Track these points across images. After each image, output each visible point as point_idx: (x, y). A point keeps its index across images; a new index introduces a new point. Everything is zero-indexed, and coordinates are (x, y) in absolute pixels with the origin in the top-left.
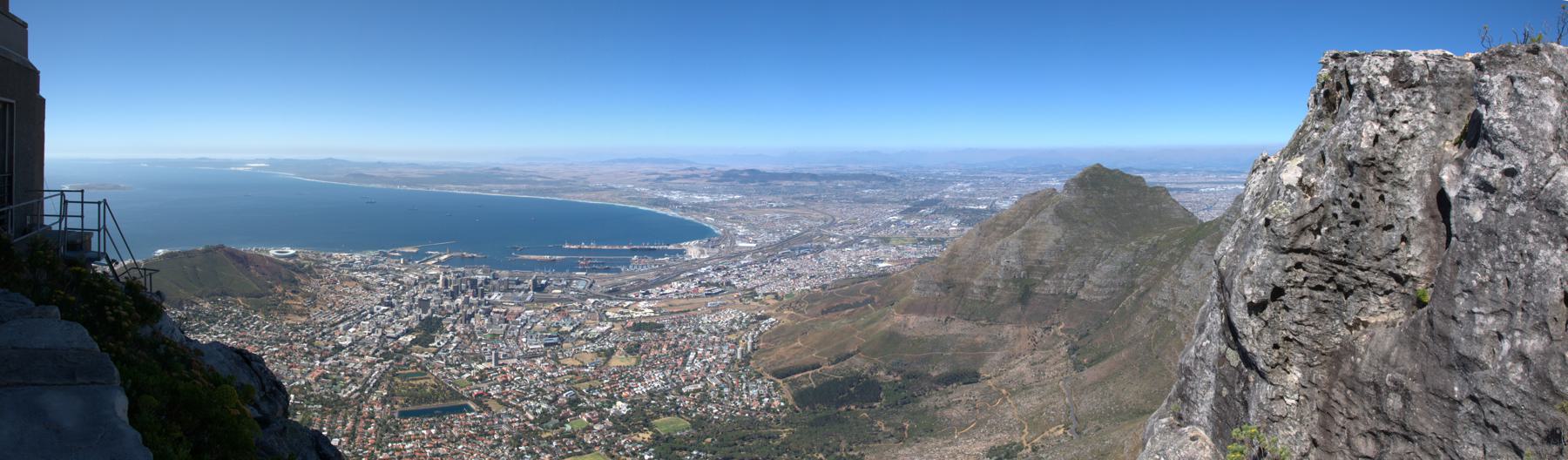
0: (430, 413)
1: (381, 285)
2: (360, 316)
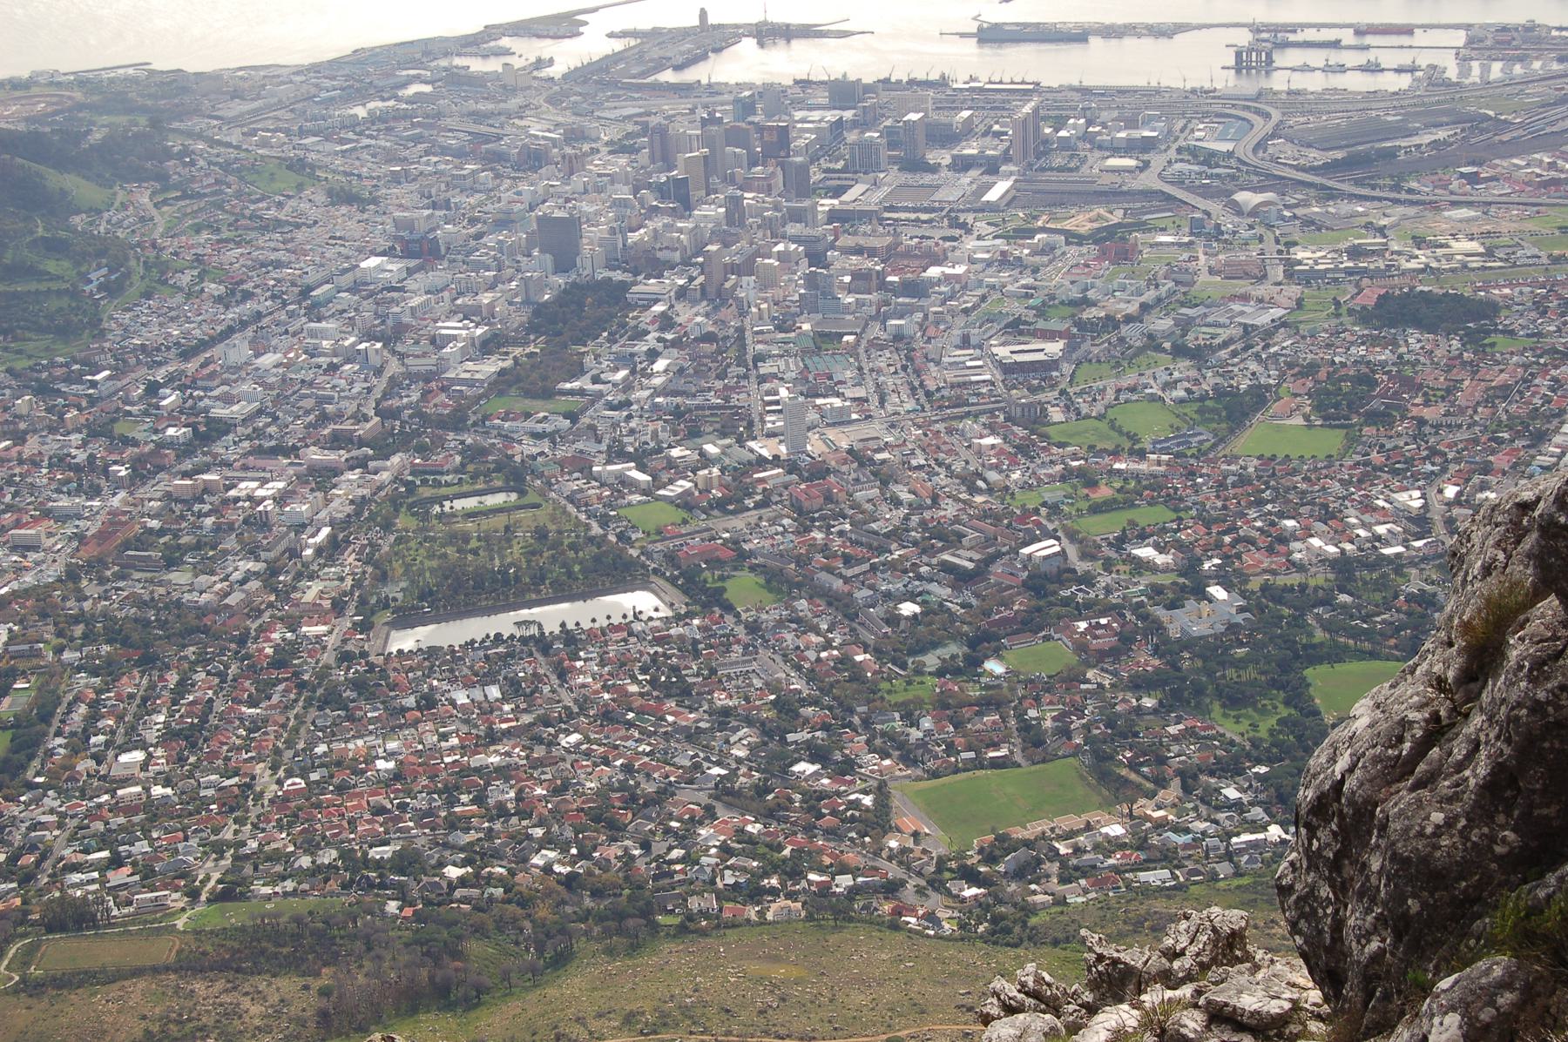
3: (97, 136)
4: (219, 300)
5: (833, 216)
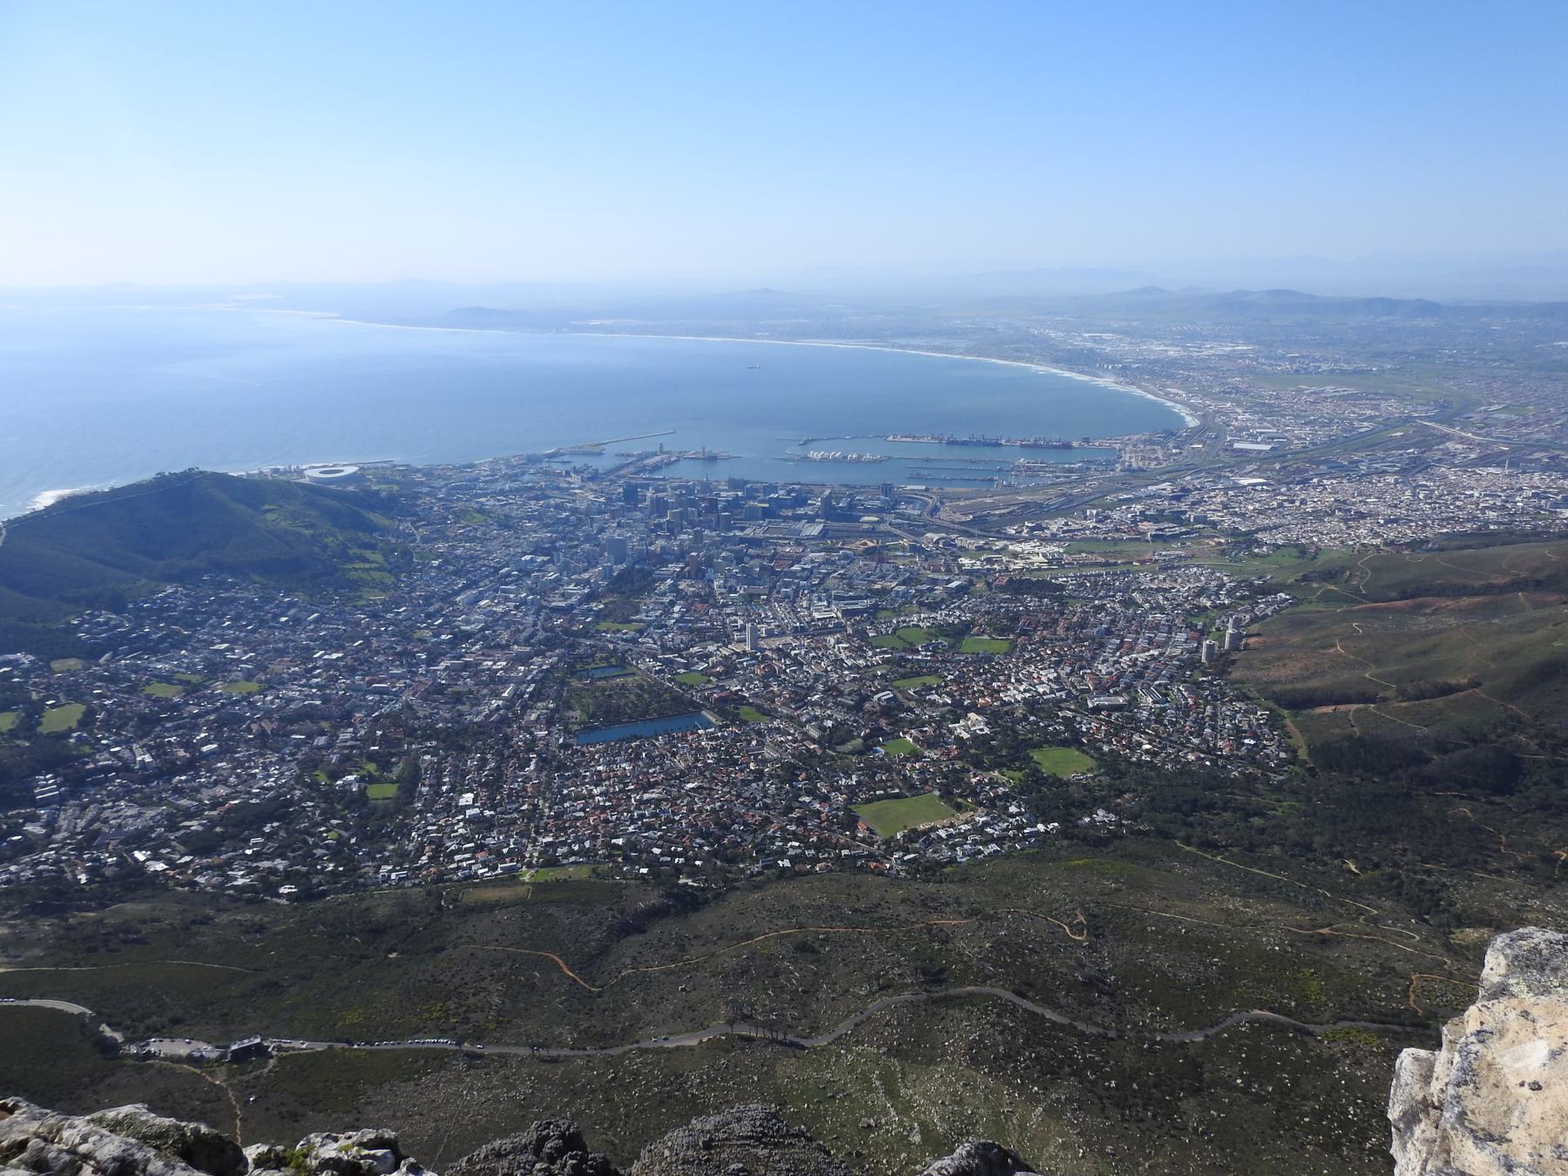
3: (384, 494)
5: (742, 540)
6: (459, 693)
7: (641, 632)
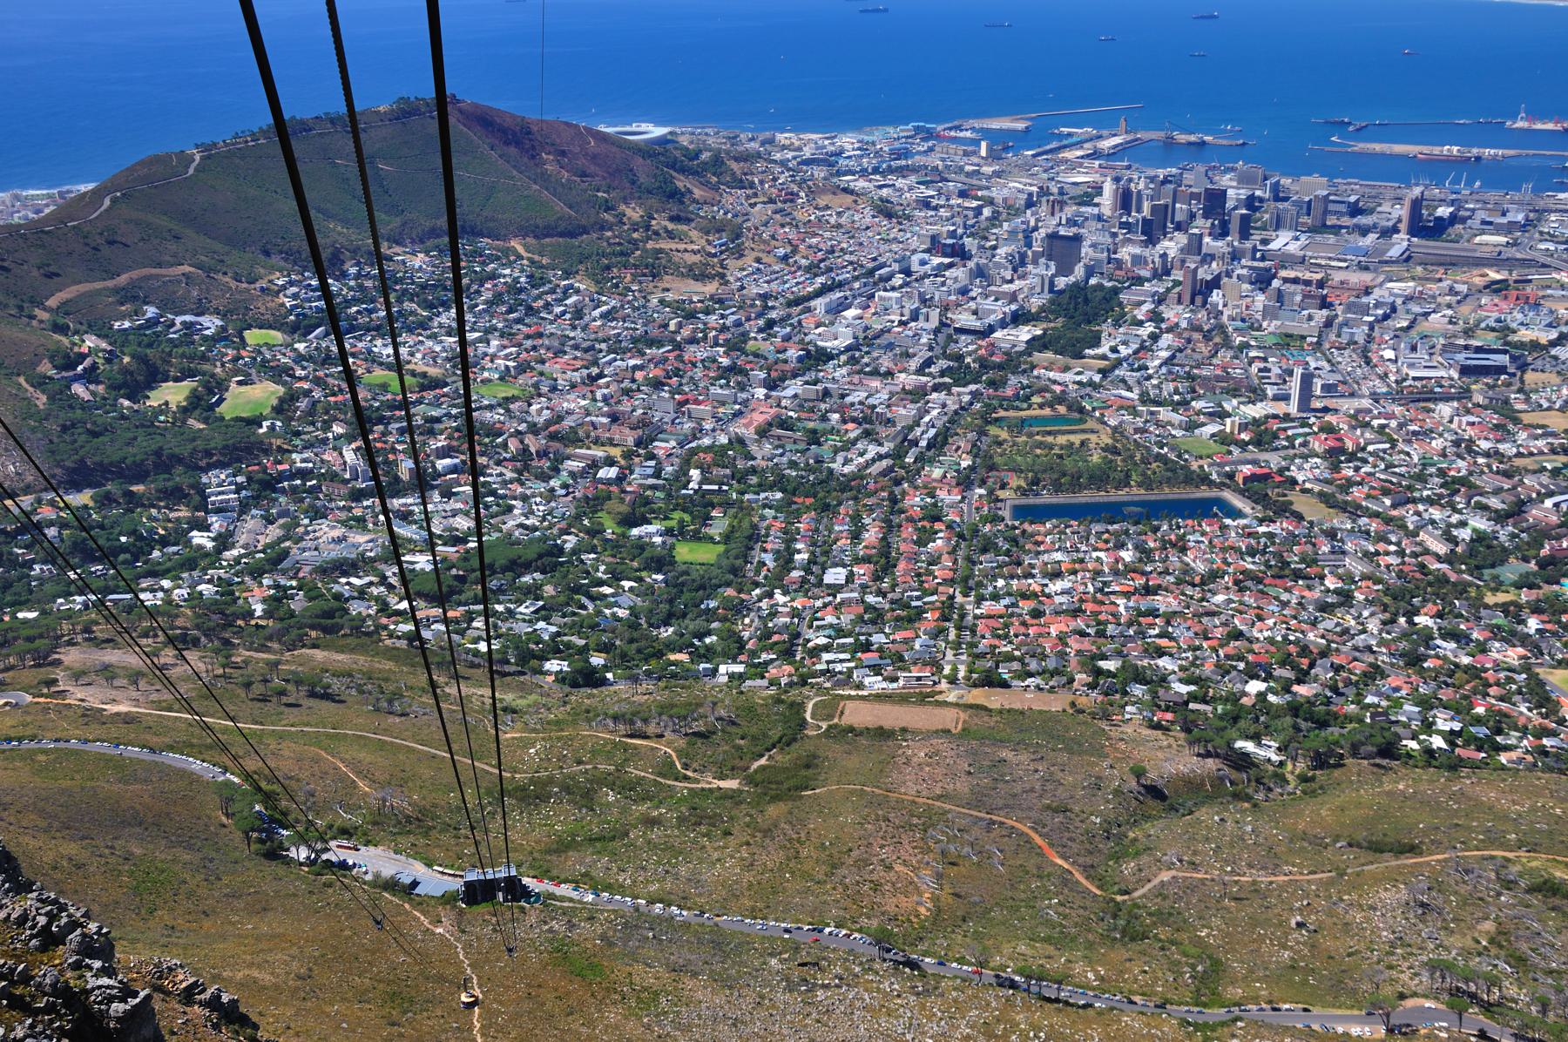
0: (1112, 512)
1: (926, 204)
2: (874, 278)
4: (808, 269)
6: (814, 432)
7: (1104, 372)
